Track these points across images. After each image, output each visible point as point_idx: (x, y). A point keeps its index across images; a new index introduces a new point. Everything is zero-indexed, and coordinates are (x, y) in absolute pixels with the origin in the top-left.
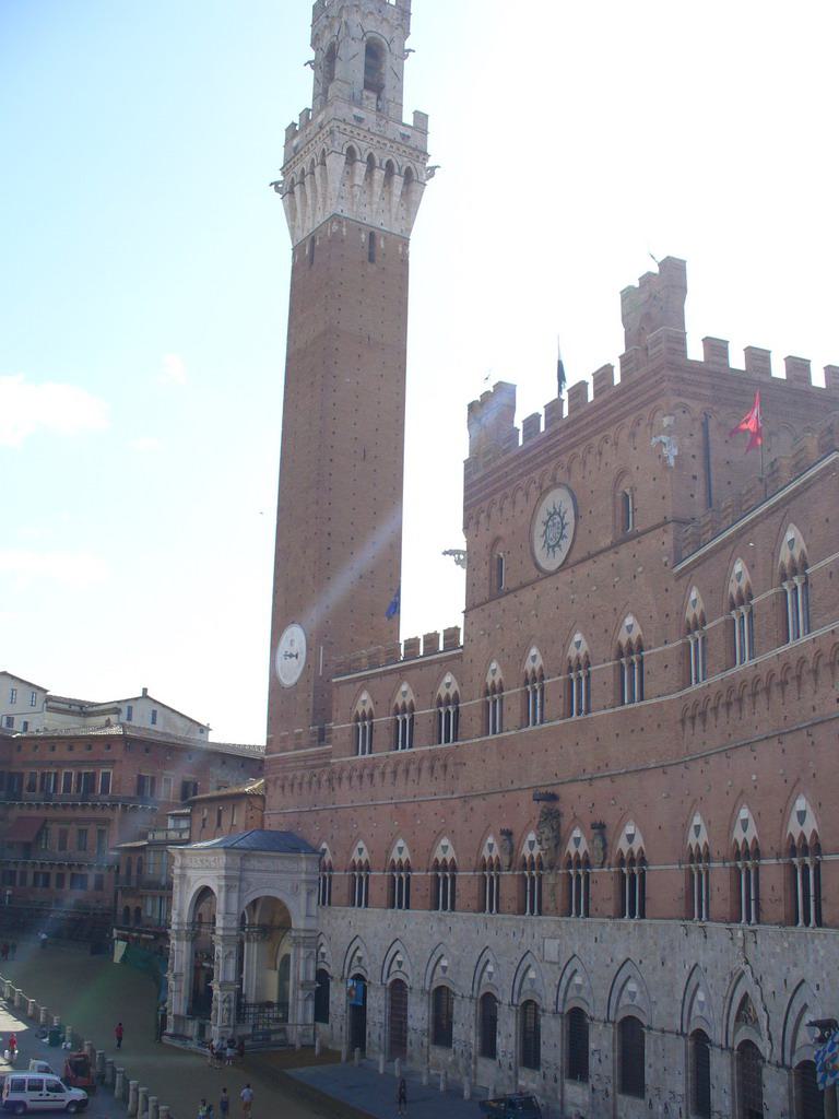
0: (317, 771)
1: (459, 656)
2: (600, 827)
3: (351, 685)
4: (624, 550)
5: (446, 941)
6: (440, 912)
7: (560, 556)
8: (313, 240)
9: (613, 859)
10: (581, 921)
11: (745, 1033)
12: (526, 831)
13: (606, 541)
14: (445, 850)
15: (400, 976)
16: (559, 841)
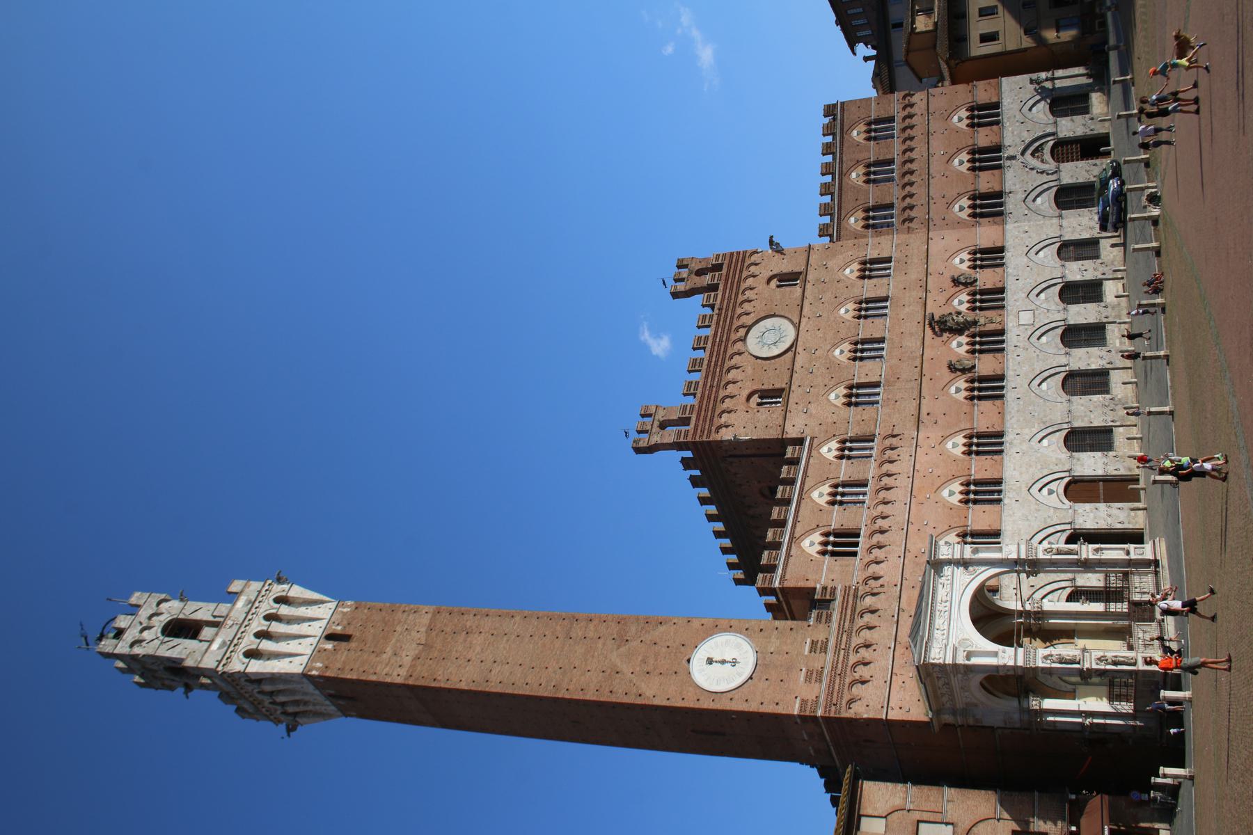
0: (858, 610)
1: (812, 439)
2: (956, 282)
3: (791, 560)
4: (810, 277)
5: (1028, 437)
6: (1006, 447)
7: (791, 333)
8: (330, 637)
9: (972, 271)
10: (1008, 295)
11: (1047, 156)
12: (951, 349)
13: (798, 290)
14: (956, 445)
15: (1061, 490)
16: (959, 313)
